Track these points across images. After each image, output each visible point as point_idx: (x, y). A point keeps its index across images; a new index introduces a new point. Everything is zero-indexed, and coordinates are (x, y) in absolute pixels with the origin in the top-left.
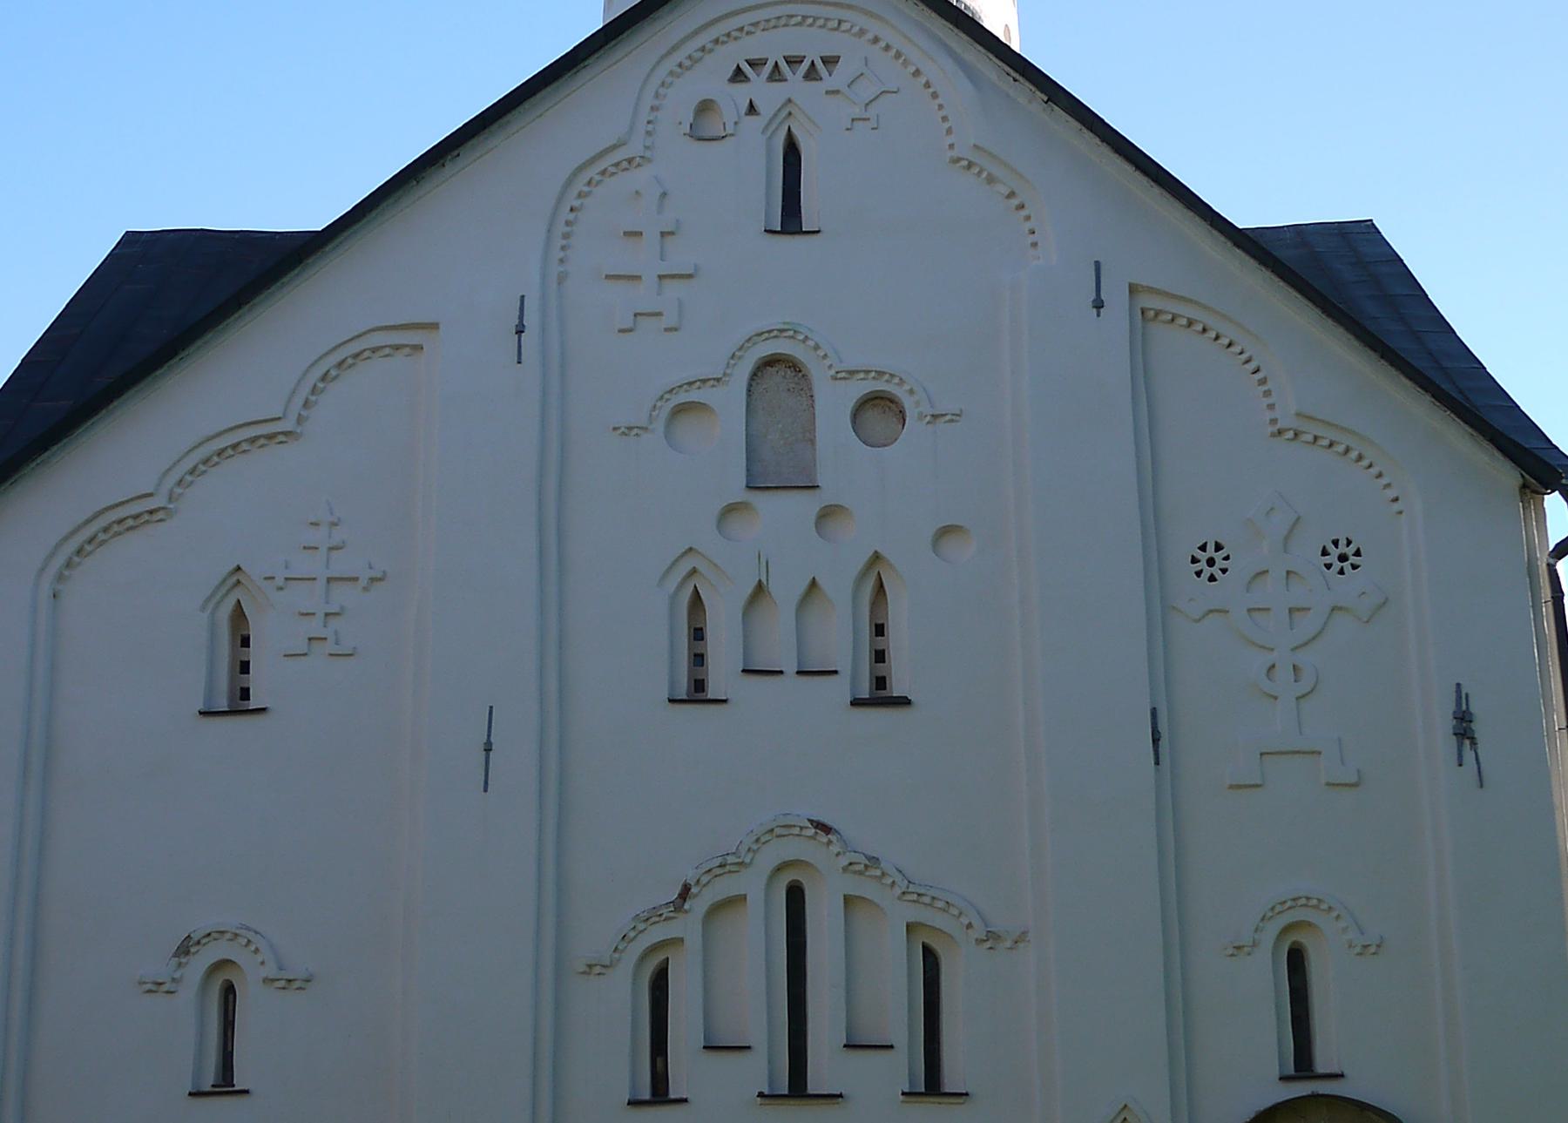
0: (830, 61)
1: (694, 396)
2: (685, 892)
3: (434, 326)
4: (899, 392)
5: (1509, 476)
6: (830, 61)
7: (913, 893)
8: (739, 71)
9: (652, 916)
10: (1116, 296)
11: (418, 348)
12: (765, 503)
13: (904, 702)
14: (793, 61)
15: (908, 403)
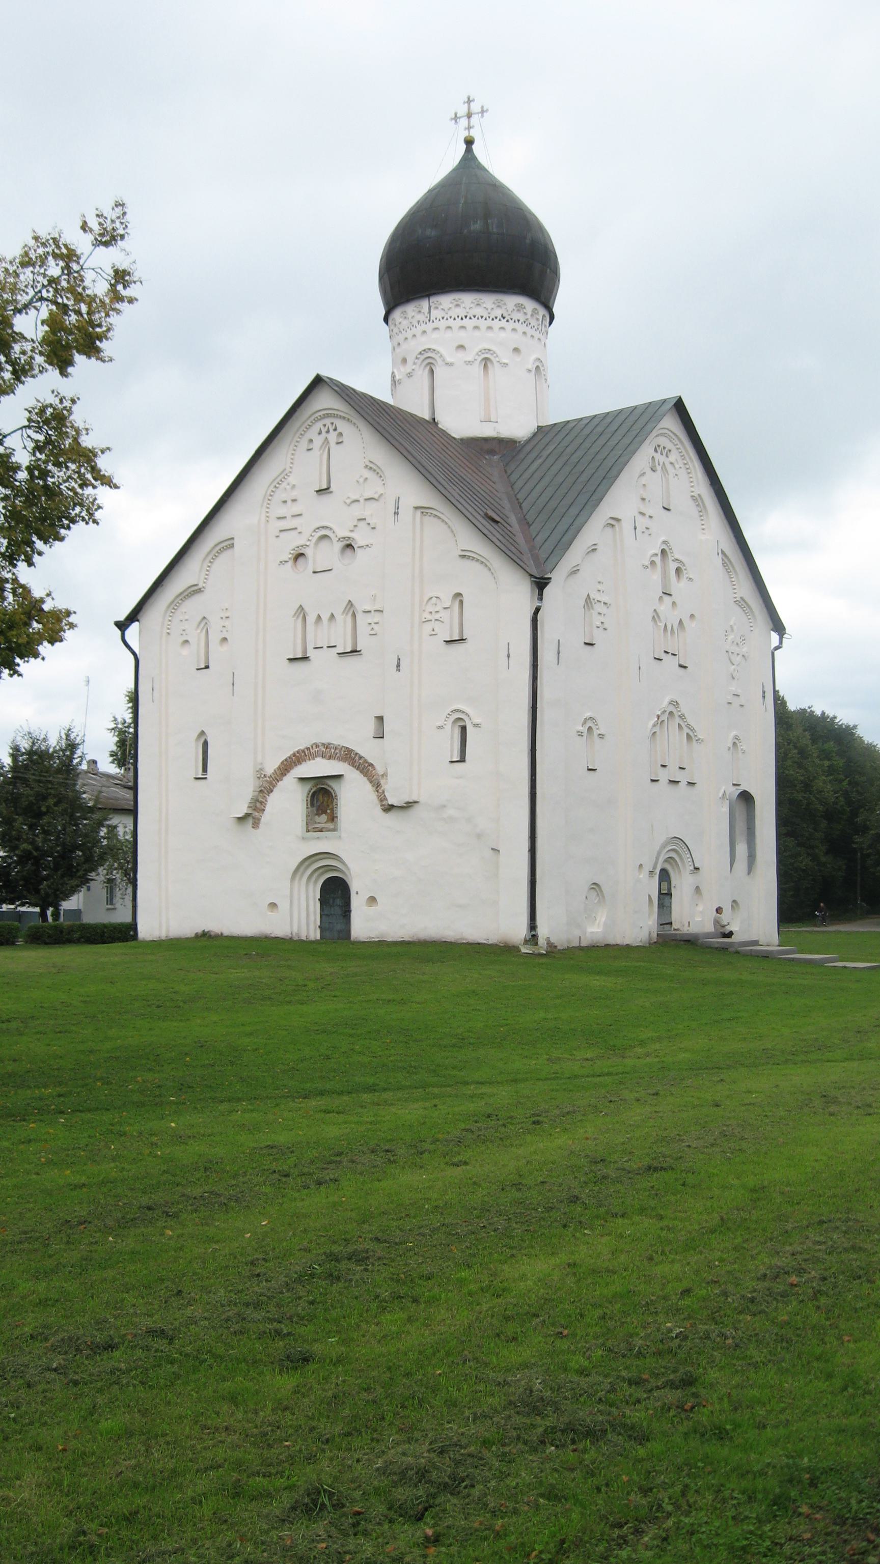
0: (670, 451)
1: (653, 558)
2: (658, 717)
3: (618, 520)
4: (683, 568)
5: (771, 626)
6: (670, 451)
7: (688, 726)
8: (655, 448)
9: (654, 726)
10: (720, 552)
11: (613, 526)
12: (666, 598)
13: (685, 667)
14: (664, 448)
15: (685, 572)
